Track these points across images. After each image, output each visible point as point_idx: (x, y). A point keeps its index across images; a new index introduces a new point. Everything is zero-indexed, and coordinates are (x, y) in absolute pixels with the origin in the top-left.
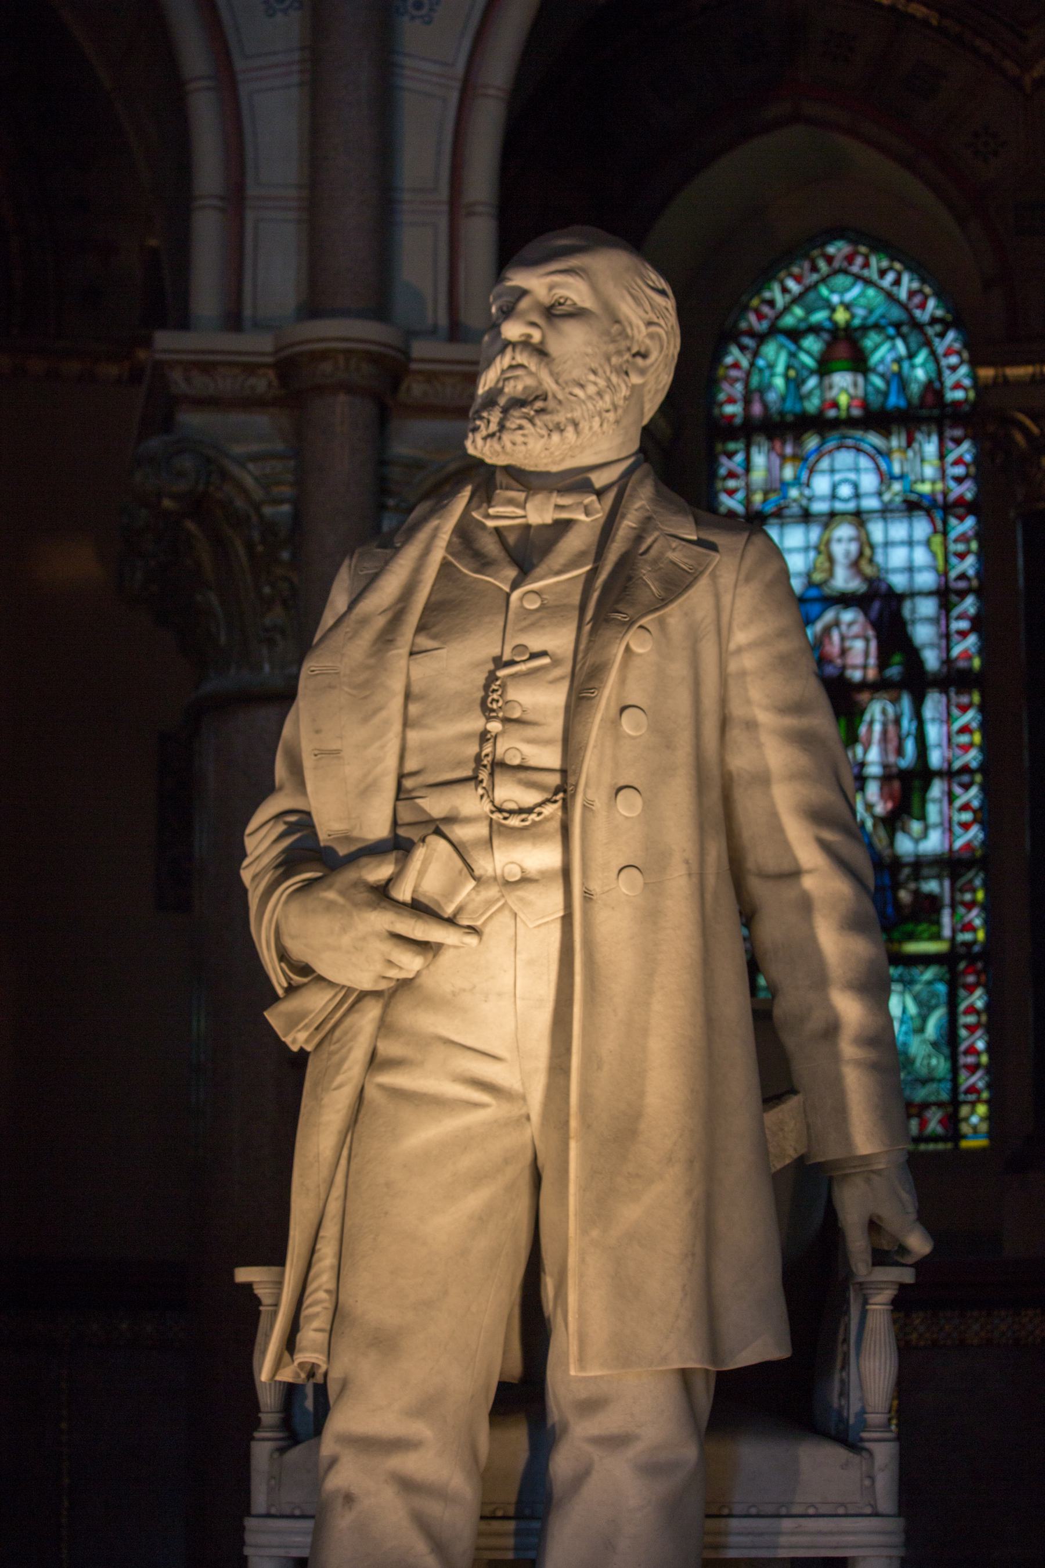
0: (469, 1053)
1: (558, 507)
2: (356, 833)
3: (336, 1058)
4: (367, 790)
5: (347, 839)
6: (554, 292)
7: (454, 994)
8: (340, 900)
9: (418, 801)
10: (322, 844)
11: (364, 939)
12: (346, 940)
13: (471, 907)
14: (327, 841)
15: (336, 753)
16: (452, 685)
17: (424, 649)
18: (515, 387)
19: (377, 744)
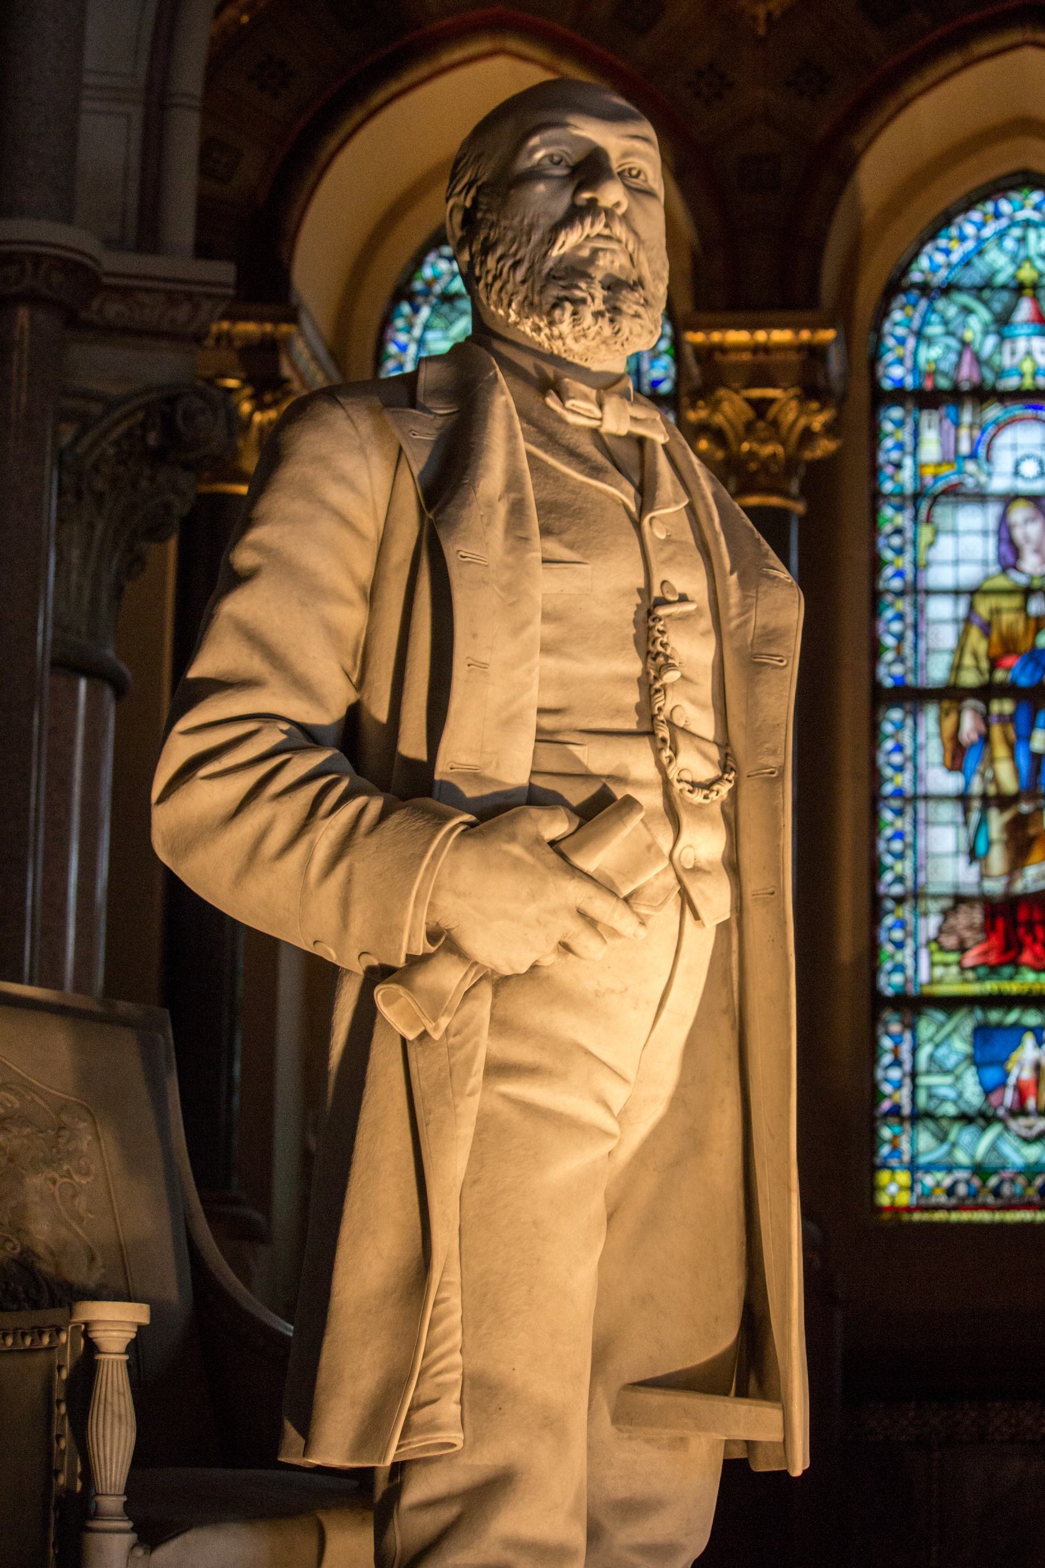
0: (606, 1069)
1: (634, 419)
2: (489, 772)
3: (460, 1056)
4: (509, 723)
5: (476, 777)
6: (630, 160)
7: (597, 994)
8: (528, 858)
9: (572, 747)
10: (437, 777)
11: (554, 912)
12: (531, 910)
13: (649, 892)
14: (447, 774)
15: (484, 666)
16: (600, 612)
17: (557, 558)
18: (612, 262)
19: (525, 666)
